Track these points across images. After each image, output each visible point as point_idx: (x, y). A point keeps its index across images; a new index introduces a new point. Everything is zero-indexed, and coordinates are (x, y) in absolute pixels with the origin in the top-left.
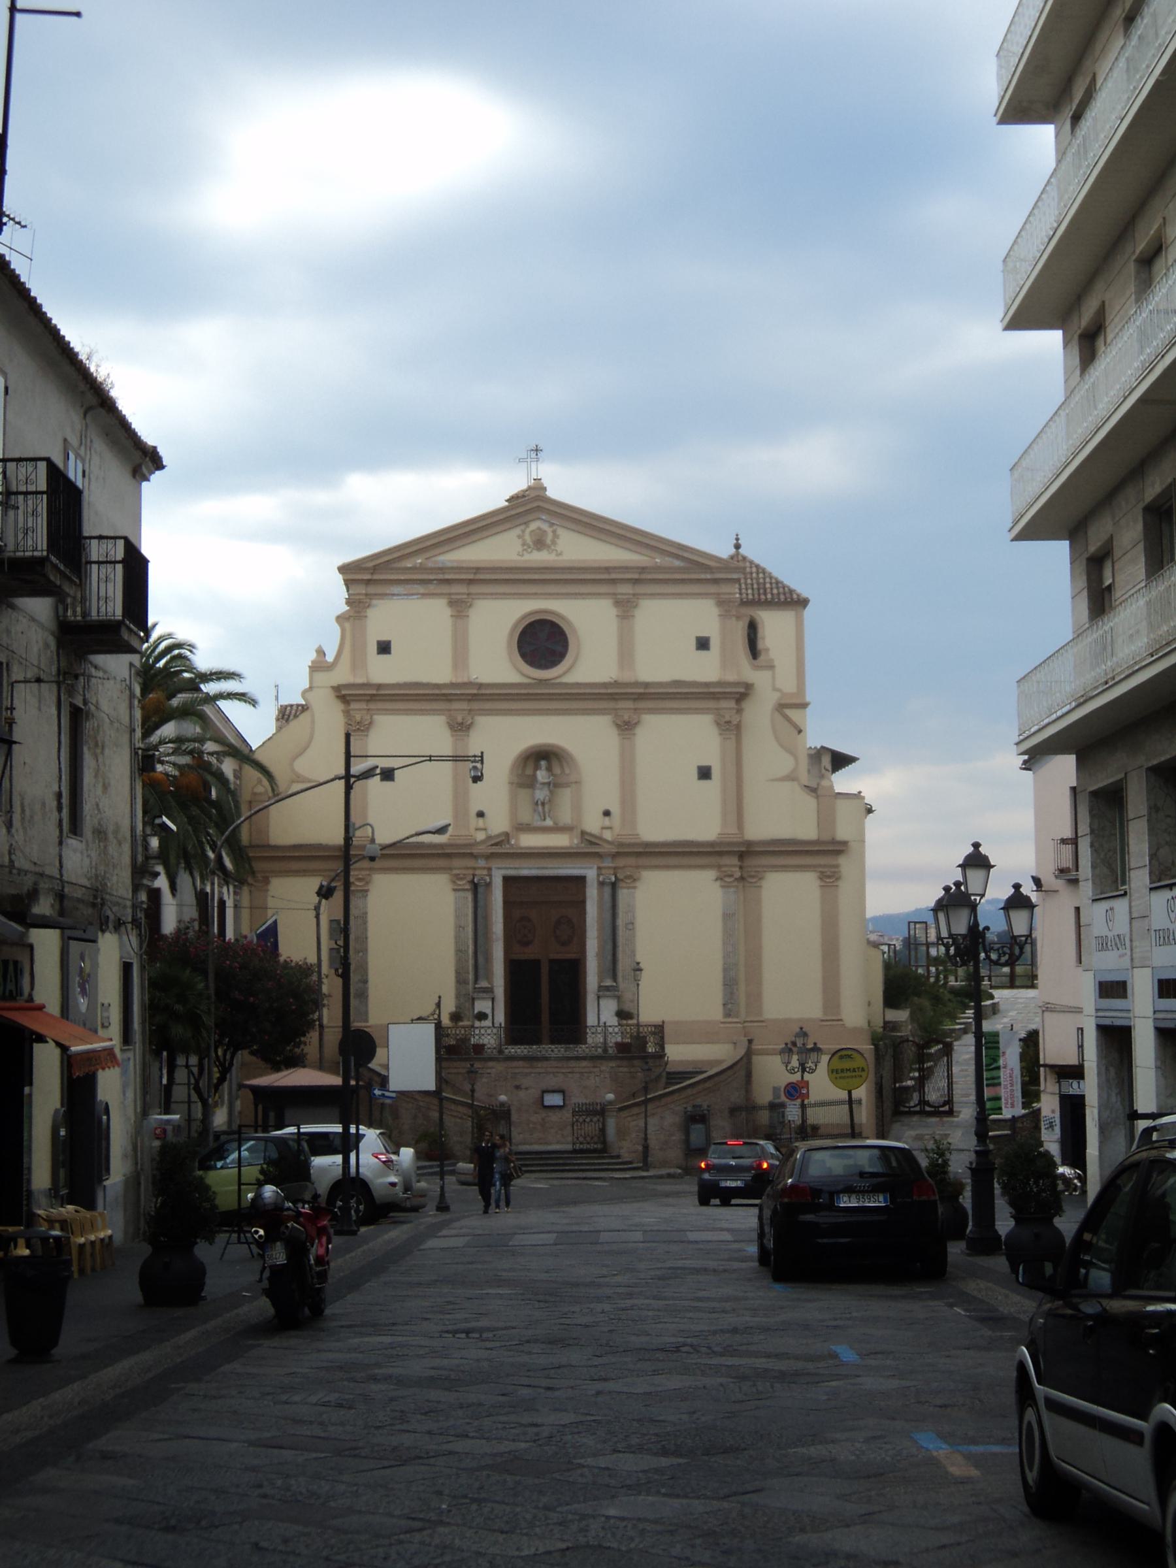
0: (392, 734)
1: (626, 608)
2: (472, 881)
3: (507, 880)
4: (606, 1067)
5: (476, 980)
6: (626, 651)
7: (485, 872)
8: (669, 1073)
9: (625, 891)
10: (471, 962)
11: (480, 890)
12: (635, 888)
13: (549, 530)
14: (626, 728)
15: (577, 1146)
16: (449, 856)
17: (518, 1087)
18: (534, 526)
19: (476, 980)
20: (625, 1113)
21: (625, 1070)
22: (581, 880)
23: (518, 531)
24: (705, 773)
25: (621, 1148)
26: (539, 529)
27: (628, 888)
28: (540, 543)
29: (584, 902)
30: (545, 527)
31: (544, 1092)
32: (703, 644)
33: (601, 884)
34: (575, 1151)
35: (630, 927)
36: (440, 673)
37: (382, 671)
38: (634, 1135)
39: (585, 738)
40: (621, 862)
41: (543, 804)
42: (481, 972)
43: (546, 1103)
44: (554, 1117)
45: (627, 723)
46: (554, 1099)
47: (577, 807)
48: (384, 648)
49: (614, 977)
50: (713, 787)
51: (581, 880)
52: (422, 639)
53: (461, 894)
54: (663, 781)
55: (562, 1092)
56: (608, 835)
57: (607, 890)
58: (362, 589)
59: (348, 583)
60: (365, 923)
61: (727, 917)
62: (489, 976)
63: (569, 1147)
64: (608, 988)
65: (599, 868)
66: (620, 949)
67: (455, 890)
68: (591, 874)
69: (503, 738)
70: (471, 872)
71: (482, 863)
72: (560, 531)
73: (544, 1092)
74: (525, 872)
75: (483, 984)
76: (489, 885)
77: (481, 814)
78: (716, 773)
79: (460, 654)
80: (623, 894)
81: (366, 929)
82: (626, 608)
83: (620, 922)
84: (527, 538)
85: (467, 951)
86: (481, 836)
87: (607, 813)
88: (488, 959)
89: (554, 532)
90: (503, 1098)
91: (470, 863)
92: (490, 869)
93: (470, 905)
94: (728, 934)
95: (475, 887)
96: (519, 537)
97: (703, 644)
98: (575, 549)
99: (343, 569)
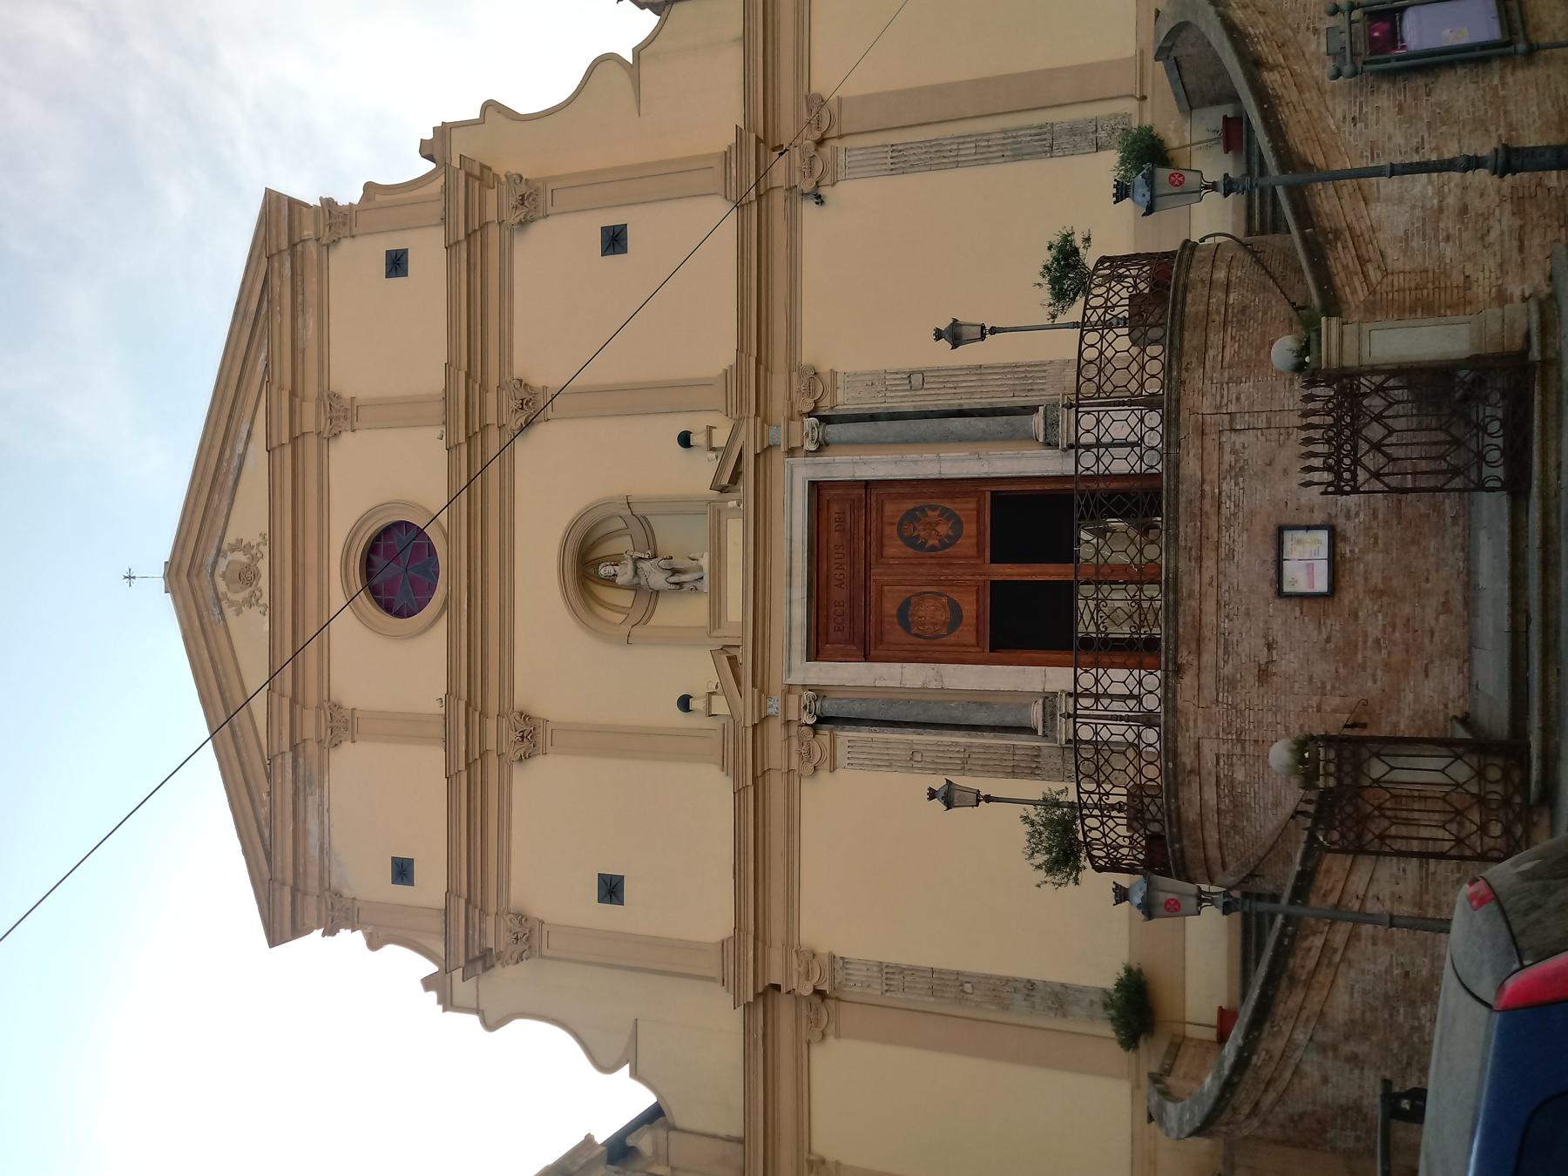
0: (545, 874)
1: (341, 415)
2: (815, 728)
3: (816, 652)
4: (1201, 399)
5: (1034, 731)
6: (397, 412)
7: (793, 700)
8: (1249, 232)
9: (840, 398)
10: (988, 740)
11: (830, 708)
12: (834, 373)
13: (231, 557)
14: (532, 408)
15: (1495, 472)
16: (760, 777)
17: (1264, 674)
18: (222, 586)
19: (1034, 731)
20: (1354, 293)
21: (1215, 338)
22: (816, 487)
23: (230, 613)
24: (614, 240)
25: (1502, 298)
26: (224, 576)
27: (835, 388)
28: (246, 576)
29: (867, 484)
30: (222, 565)
31: (1280, 593)
32: (397, 264)
33: (822, 446)
34: (1516, 487)
35: (917, 379)
36: (425, 769)
37: (431, 885)
38: (1449, 251)
39: (552, 485)
40: (778, 407)
41: (675, 572)
42: (1010, 720)
43: (1321, 585)
44: (1371, 564)
45: (523, 404)
46: (1307, 563)
47: (679, 506)
48: (403, 871)
49: (1031, 410)
50: (641, 225)
51: (816, 487)
52: (387, 798)
53: (841, 752)
54: (624, 323)
55: (1280, 530)
56: (720, 439)
57: (834, 431)
58: (311, 901)
59: (297, 931)
60: (901, 970)
61: (900, 162)
62: (1021, 698)
63: (1493, 508)
64: (1051, 425)
65: (791, 452)
66: (968, 403)
67: (833, 769)
68: (803, 472)
69: (555, 655)
70: (794, 729)
71: (774, 707)
72: (230, 538)
73: (1280, 593)
74: (800, 613)
75: (1036, 715)
76: (819, 692)
77: (684, 703)
78: (613, 219)
79: (398, 728)
80: (846, 401)
81: (914, 970)
82: (341, 415)
83: (906, 406)
84: (239, 597)
85: (970, 746)
86: (720, 706)
87: (685, 440)
88: (982, 699)
89: (233, 549)
90: (1279, 754)
91: (775, 731)
92: (789, 689)
93: (863, 734)
94: (940, 157)
95: (823, 720)
96: (239, 612)
97: (397, 264)
98: (249, 517)
99: (274, 938)
